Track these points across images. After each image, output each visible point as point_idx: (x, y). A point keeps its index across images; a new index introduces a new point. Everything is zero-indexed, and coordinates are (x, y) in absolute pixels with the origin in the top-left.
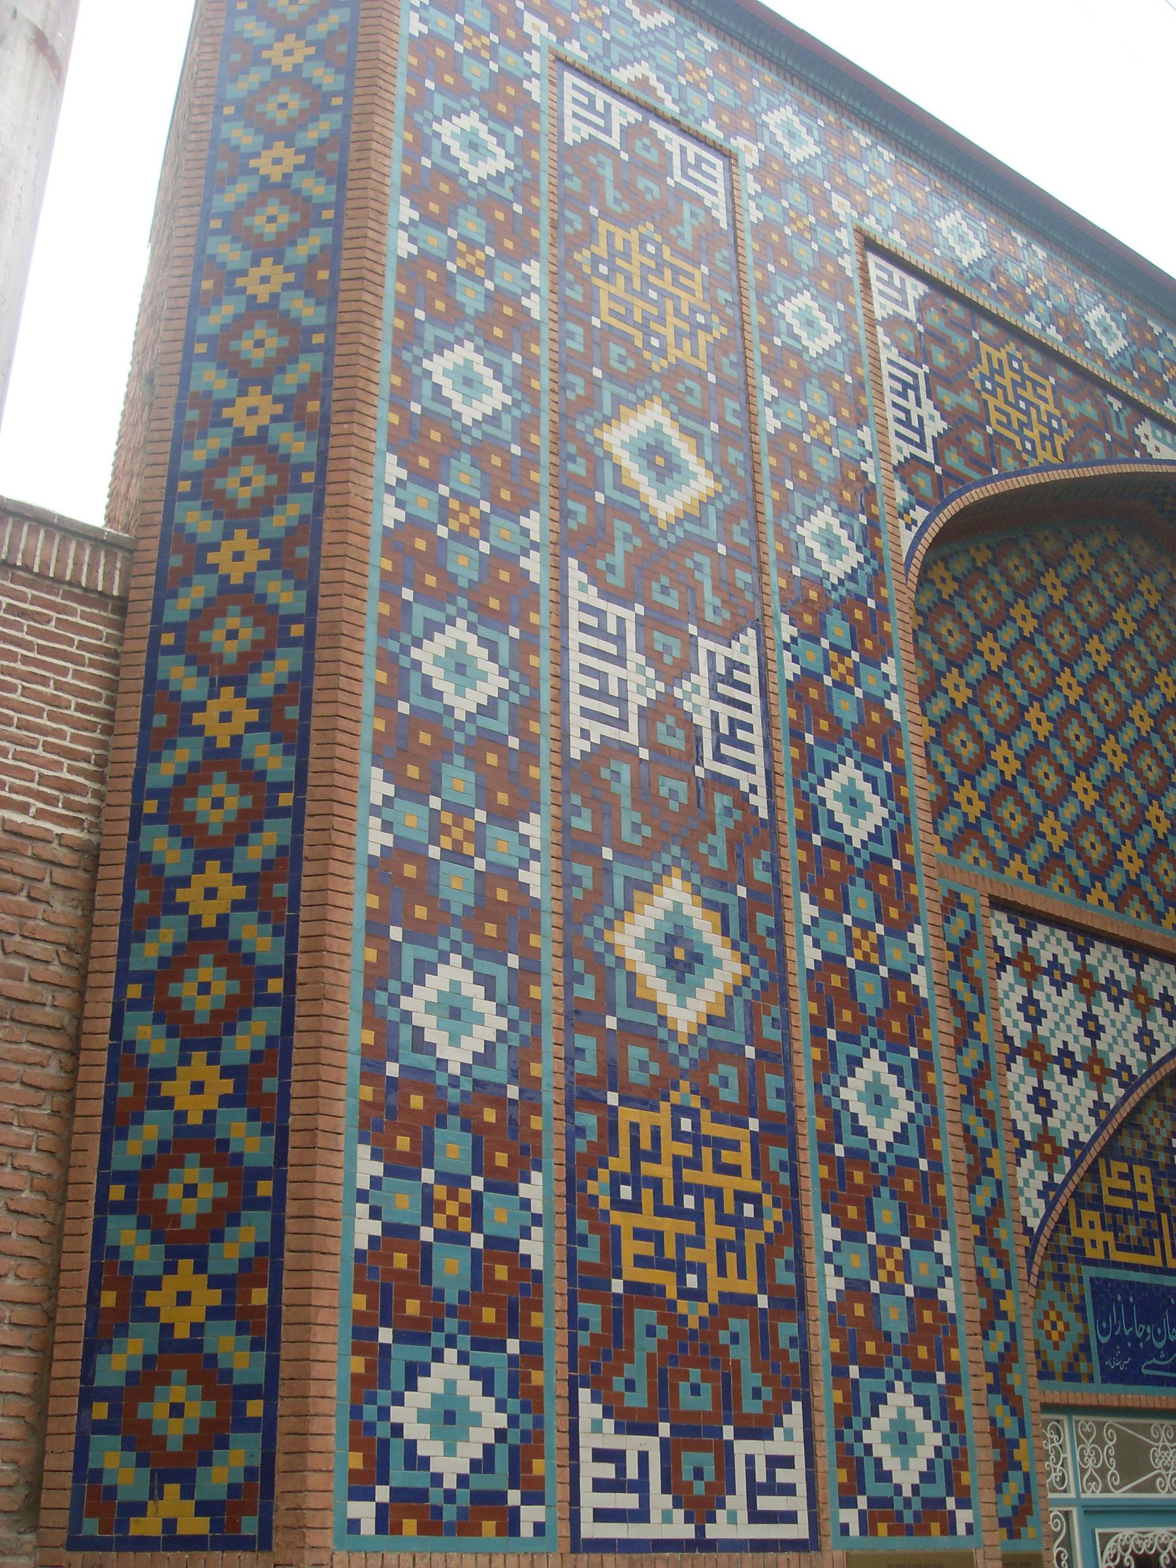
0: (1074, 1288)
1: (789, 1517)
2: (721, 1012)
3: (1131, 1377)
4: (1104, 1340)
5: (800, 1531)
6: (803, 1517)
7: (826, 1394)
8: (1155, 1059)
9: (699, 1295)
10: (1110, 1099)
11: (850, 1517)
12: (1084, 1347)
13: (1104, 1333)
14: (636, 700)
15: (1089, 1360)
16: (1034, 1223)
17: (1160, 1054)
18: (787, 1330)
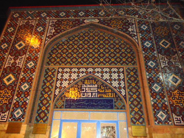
0: (63, 100)
1: (5, 119)
2: (5, 83)
3: (70, 108)
4: (66, 104)
5: (5, 120)
6: (6, 120)
7: (11, 110)
8: (79, 78)
9: (2, 103)
10: (71, 82)
11: (10, 120)
12: (63, 105)
13: (66, 104)
14: (12, 62)
15: (63, 106)
16: (57, 94)
17: (80, 77)
18: (9, 105)
